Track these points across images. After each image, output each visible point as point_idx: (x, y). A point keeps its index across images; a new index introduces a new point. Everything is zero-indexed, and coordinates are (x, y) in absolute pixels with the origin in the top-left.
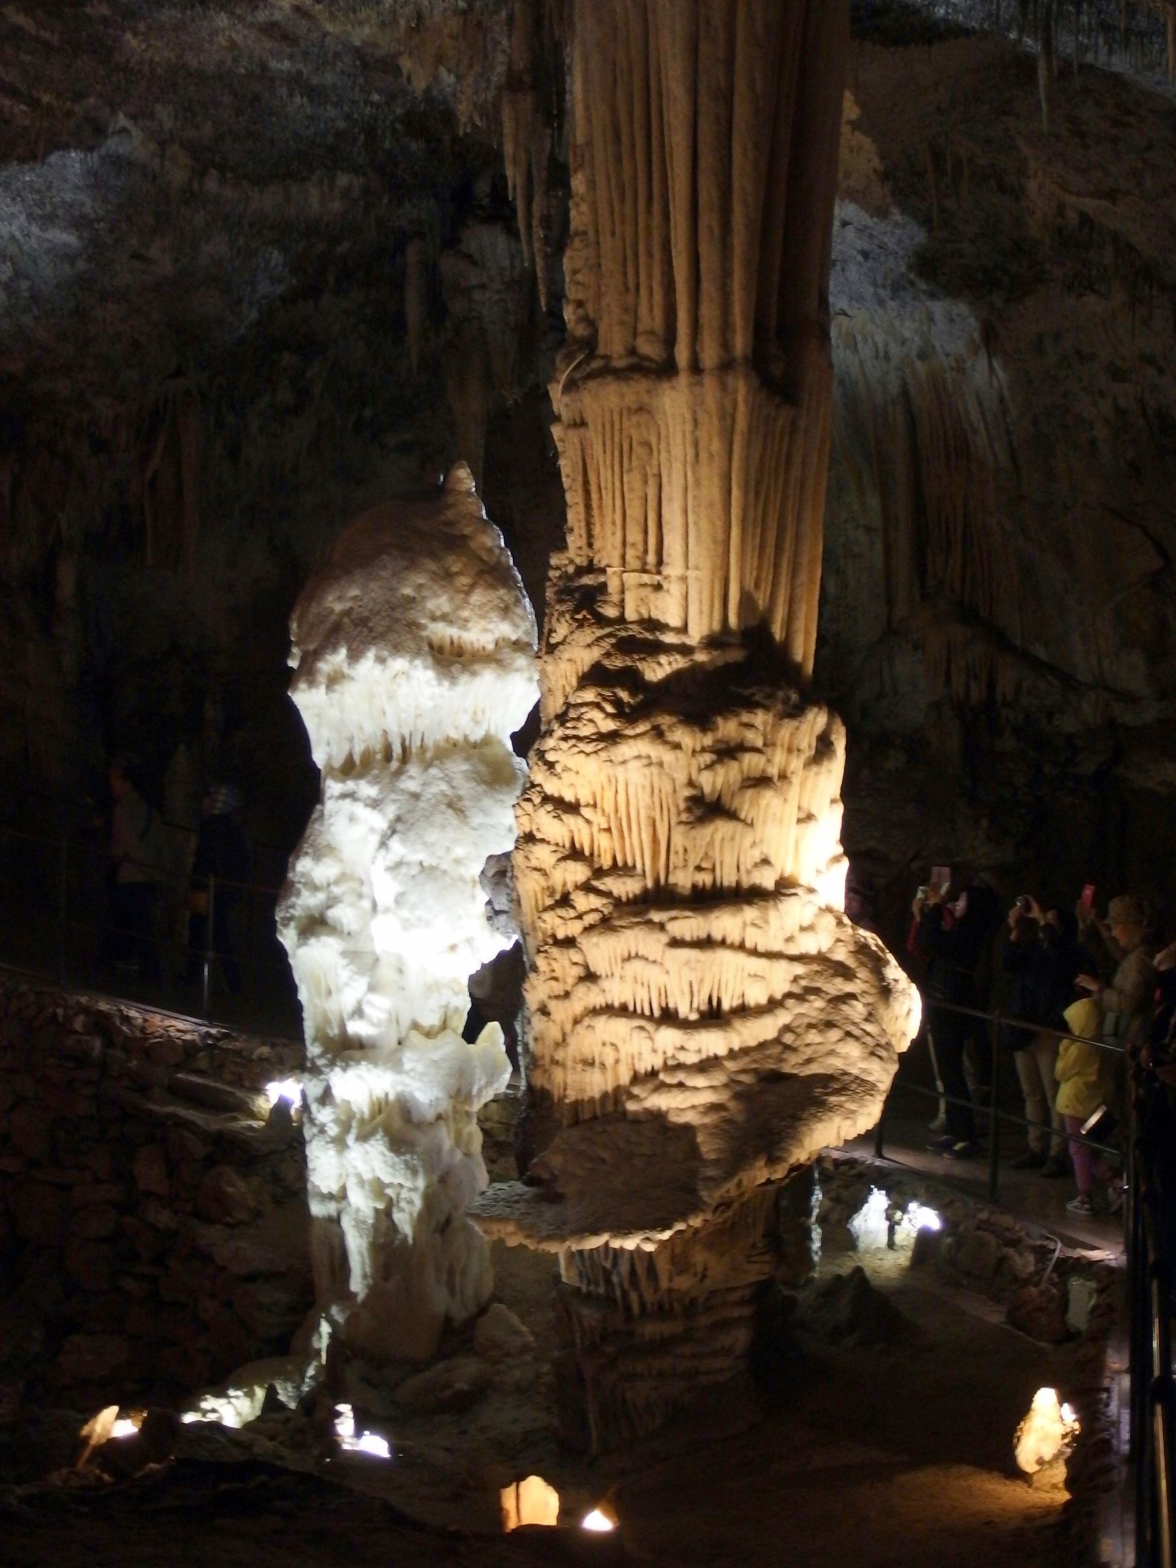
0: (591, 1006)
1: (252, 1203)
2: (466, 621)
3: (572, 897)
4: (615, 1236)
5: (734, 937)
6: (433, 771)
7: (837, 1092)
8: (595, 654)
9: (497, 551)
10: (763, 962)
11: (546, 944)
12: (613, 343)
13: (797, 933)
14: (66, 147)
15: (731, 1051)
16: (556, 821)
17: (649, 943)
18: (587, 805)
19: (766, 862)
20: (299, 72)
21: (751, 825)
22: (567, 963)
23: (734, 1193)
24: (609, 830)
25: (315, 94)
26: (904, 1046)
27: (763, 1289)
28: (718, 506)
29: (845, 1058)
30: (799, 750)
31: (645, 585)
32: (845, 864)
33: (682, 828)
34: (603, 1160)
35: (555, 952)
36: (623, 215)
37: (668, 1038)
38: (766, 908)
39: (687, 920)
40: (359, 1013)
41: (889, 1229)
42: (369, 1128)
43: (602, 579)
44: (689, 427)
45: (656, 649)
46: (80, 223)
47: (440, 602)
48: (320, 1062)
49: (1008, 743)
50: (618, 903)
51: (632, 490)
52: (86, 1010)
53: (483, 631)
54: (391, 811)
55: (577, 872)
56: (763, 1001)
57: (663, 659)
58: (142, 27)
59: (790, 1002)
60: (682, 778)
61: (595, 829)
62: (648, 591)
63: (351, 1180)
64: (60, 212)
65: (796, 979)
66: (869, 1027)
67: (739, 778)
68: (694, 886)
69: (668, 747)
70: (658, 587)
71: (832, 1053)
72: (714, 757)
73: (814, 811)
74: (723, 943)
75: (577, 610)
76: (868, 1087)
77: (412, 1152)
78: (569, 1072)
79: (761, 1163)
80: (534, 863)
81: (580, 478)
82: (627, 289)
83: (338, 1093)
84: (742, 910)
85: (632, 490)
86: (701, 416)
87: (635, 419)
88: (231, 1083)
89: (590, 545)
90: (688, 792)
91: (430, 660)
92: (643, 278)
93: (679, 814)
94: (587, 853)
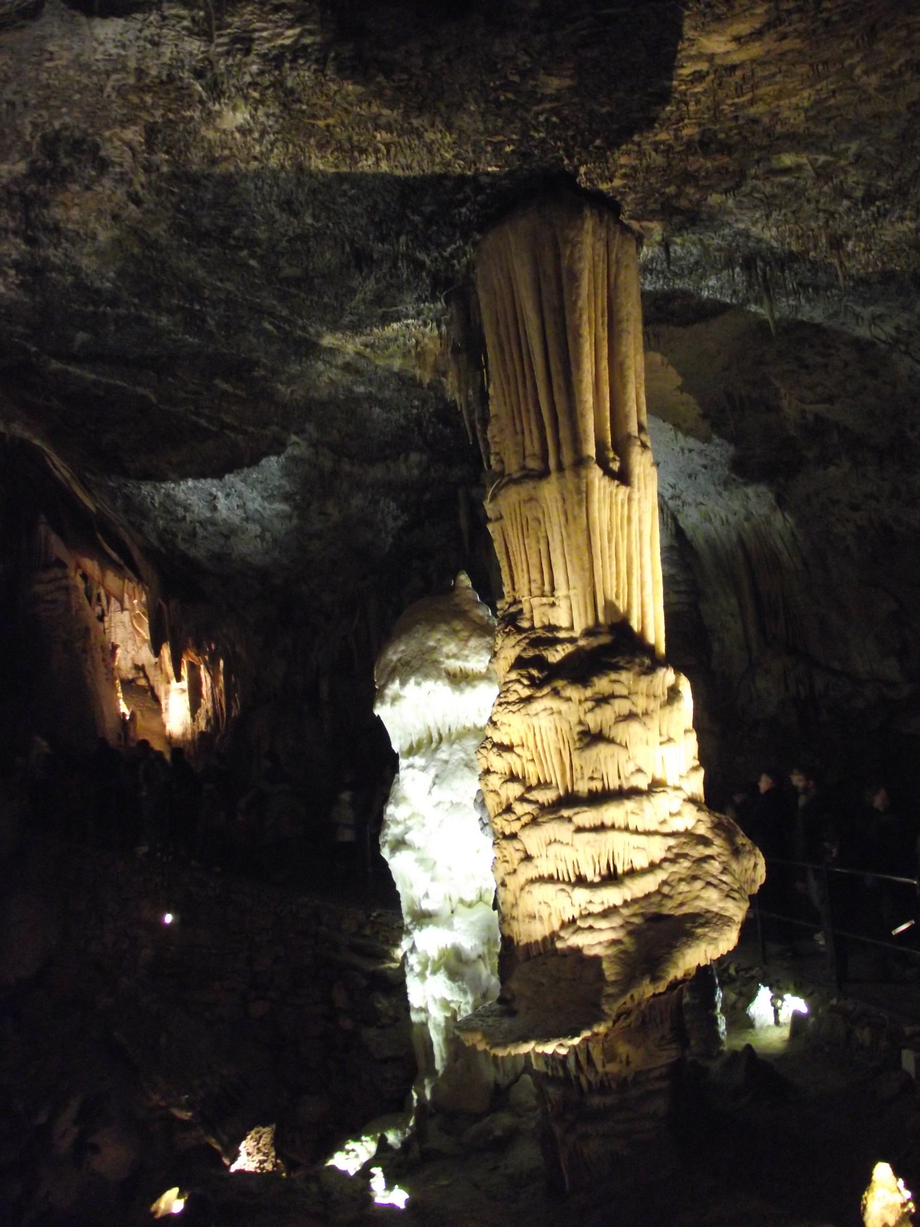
0: (530, 878)
5: (620, 822)
6: (455, 746)
7: (702, 925)
8: (518, 650)
10: (643, 839)
11: (498, 838)
12: (512, 466)
13: (668, 817)
15: (625, 902)
16: (499, 758)
18: (518, 746)
19: (639, 770)
20: (371, 393)
21: (626, 747)
22: (512, 851)
23: (629, 1005)
24: (533, 760)
25: (381, 403)
28: (584, 548)
30: (655, 697)
31: (544, 605)
35: (504, 843)
37: (581, 895)
38: (641, 801)
39: (584, 814)
42: (437, 966)
43: (520, 606)
44: (560, 504)
45: (554, 642)
46: (287, 498)
47: (451, 647)
48: (410, 927)
53: (478, 662)
54: (432, 772)
55: (515, 790)
56: (646, 865)
57: (559, 648)
58: (284, 378)
60: (574, 720)
61: (524, 761)
62: (547, 608)
64: (275, 493)
67: (613, 716)
68: (590, 791)
69: (562, 700)
70: (553, 605)
74: (613, 827)
76: (726, 920)
77: (462, 980)
78: (521, 924)
79: (646, 981)
80: (491, 787)
81: (504, 550)
82: (517, 433)
83: (419, 947)
86: (567, 496)
87: (528, 505)
89: (514, 589)
90: (579, 728)
91: (446, 681)
92: (525, 425)
93: (575, 742)
94: (521, 777)
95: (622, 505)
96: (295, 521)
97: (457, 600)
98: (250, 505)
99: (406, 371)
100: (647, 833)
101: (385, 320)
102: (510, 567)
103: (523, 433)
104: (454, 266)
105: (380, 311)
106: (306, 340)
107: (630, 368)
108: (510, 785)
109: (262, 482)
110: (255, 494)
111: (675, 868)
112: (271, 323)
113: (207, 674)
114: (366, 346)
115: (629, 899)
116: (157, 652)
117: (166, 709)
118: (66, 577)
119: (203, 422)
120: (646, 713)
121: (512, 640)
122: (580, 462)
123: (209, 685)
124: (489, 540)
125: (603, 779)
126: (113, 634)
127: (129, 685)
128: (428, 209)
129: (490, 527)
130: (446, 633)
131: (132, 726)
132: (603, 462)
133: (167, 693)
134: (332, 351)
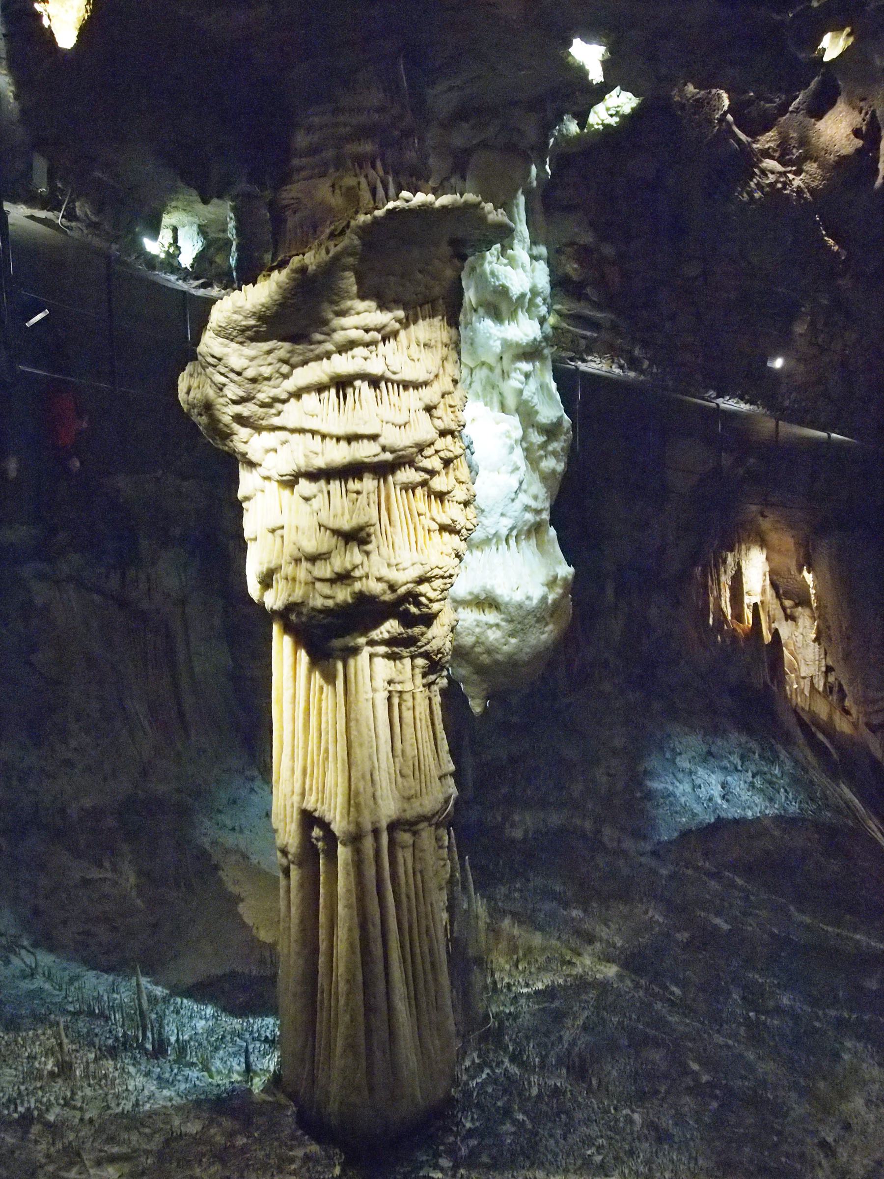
0: (428, 387)
1: (563, 258)
2: (478, 626)
3: (442, 466)
4: (432, 204)
5: (330, 443)
6: (493, 532)
7: (248, 328)
8: (430, 633)
9: (454, 665)
10: (307, 427)
11: (459, 431)
12: (427, 834)
13: (279, 448)
14: (670, 842)
15: (329, 358)
19: (307, 499)
21: (320, 526)
22: (445, 418)
23: (331, 244)
24: (419, 515)
25: (550, 895)
27: (284, 179)
28: (355, 744)
29: (242, 355)
30: (287, 579)
31: (399, 683)
32: (240, 495)
33: (373, 522)
34: (420, 271)
35: (454, 426)
36: (427, 918)
37: (375, 367)
38: (307, 466)
40: (527, 376)
41: (178, 237)
44: (378, 793)
46: (649, 795)
47: (493, 636)
48: (544, 344)
50: (411, 463)
51: (412, 745)
52: (642, 372)
55: (438, 484)
56: (305, 396)
57: (386, 636)
59: (284, 396)
60: (374, 556)
61: (428, 515)
62: (397, 679)
63: (520, 269)
64: (662, 800)
65: (279, 413)
66: (222, 379)
67: (333, 559)
68: (361, 479)
69: (386, 579)
70: (390, 682)
71: (252, 359)
72: (352, 574)
73: (270, 534)
77: (495, 287)
78: (439, 339)
79: (312, 268)
80: (464, 487)
81: (439, 743)
82: (421, 872)
83: (536, 324)
84: (326, 465)
85: (412, 745)
86: (372, 802)
87: (413, 792)
88: (569, 331)
89: (430, 699)
90: (369, 547)
91: (500, 600)
93: (375, 533)
94: (433, 497)
95: (311, 789)
96: (641, 769)
98: (687, 787)
100: (302, 431)
101: (549, 993)
102: (433, 724)
103: (414, 873)
105: (556, 1004)
107: (296, 941)
108: (445, 490)
109: (676, 812)
111: (274, 392)
113: (725, 609)
114: (570, 963)
115: (325, 359)
116: (776, 634)
117: (765, 575)
118: (867, 714)
119: (740, 882)
120: (297, 561)
121: (434, 645)
122: (355, 839)
123: (723, 599)
124: (454, 753)
125: (347, 491)
126: (817, 653)
127: (803, 601)
128: (508, 1127)
129: (452, 767)
130: (497, 650)
131: (801, 560)
132: (330, 837)
133: (764, 592)
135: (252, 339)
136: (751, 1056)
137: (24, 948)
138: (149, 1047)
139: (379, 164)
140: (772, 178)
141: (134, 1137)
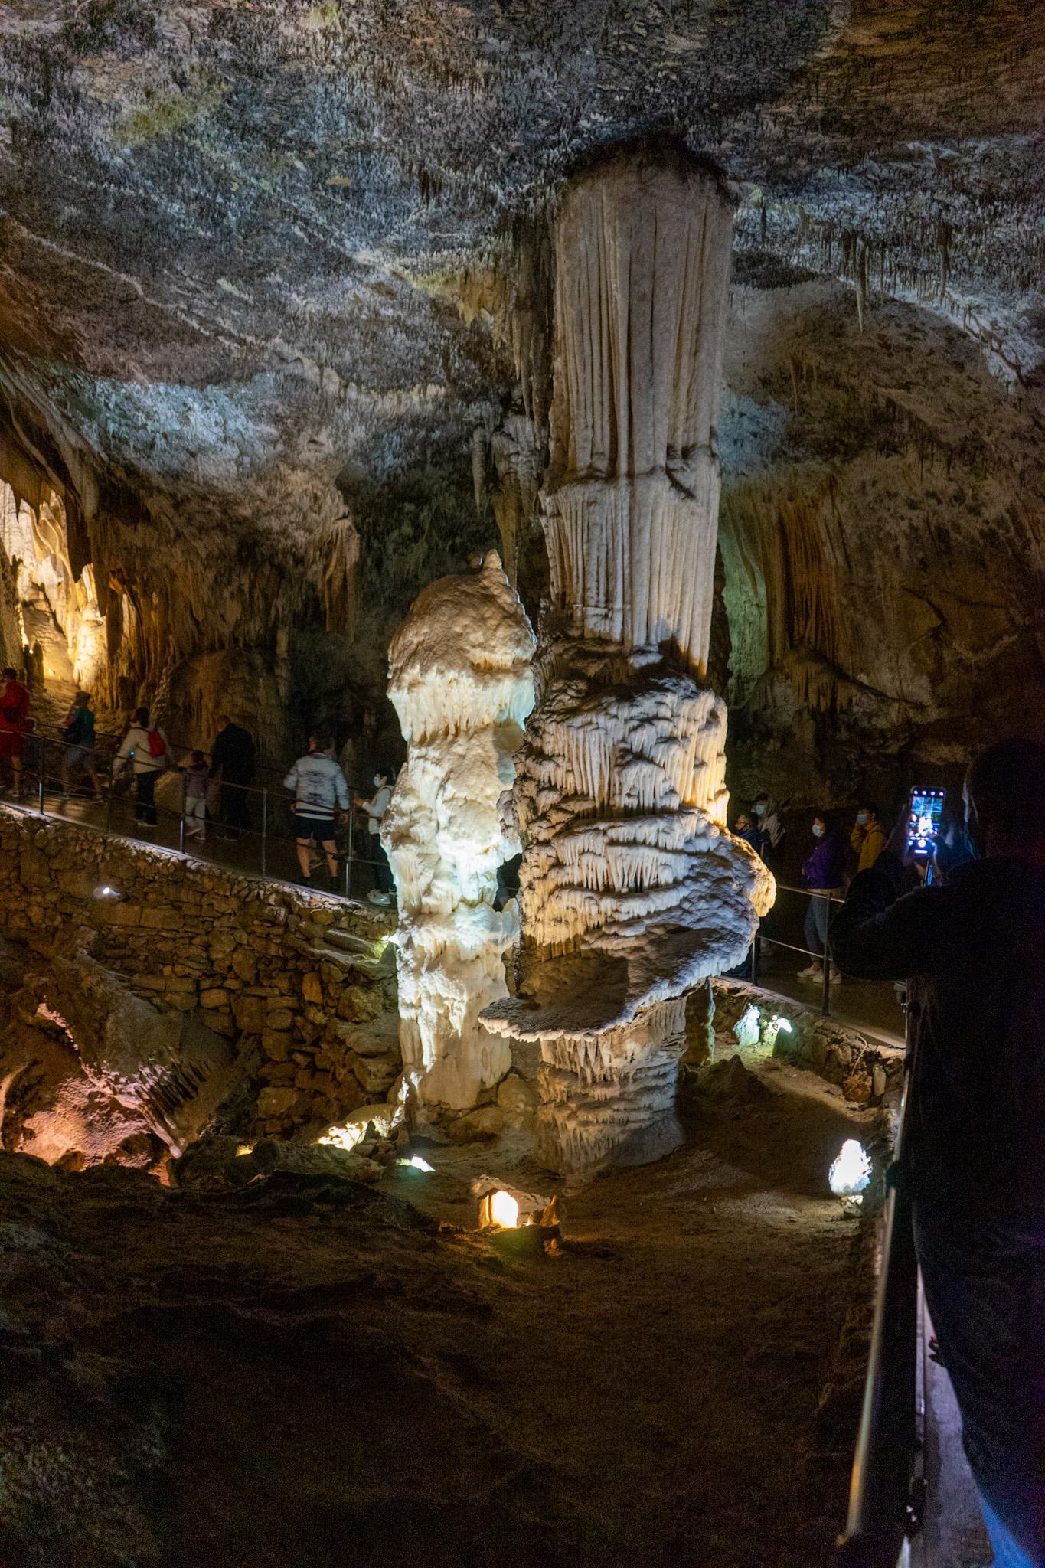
4: (567, 1032)
5: (652, 839)
6: (473, 741)
7: (717, 940)
10: (670, 856)
17: (597, 843)
19: (672, 791)
20: (399, 317)
25: (408, 330)
26: (764, 912)
35: (536, 849)
37: (608, 904)
47: (477, 636)
48: (406, 922)
49: (844, 735)
52: (277, 892)
54: (447, 766)
56: (670, 881)
58: (302, 288)
59: (688, 882)
65: (693, 867)
71: (714, 915)
75: (554, 632)
83: (416, 941)
90: (622, 745)
91: (471, 672)
97: (486, 582)
98: (231, 425)
99: (444, 298)
100: (675, 852)
104: (527, 203)
105: (431, 235)
106: (340, 254)
110: (239, 411)
112: (301, 229)
119: (194, 323)
120: (685, 737)
128: (513, 145)
134: (366, 269)
135: (714, 931)
136: (234, 165)
137: (977, 335)
138: (859, 242)
139: (589, 1080)
140: (131, 1088)
141: (884, 173)
